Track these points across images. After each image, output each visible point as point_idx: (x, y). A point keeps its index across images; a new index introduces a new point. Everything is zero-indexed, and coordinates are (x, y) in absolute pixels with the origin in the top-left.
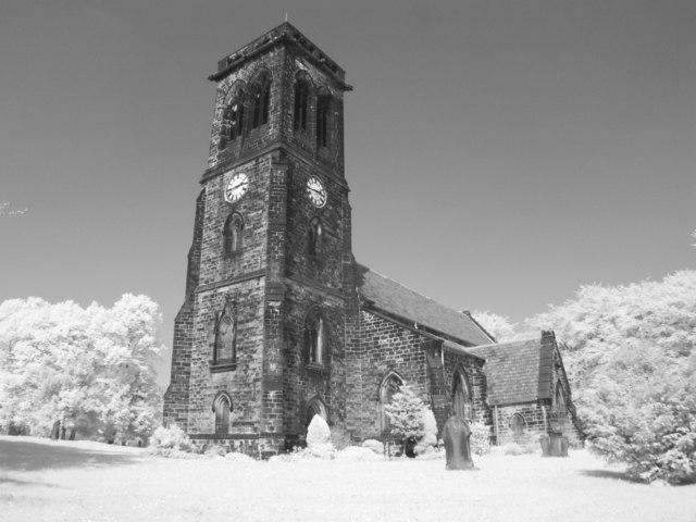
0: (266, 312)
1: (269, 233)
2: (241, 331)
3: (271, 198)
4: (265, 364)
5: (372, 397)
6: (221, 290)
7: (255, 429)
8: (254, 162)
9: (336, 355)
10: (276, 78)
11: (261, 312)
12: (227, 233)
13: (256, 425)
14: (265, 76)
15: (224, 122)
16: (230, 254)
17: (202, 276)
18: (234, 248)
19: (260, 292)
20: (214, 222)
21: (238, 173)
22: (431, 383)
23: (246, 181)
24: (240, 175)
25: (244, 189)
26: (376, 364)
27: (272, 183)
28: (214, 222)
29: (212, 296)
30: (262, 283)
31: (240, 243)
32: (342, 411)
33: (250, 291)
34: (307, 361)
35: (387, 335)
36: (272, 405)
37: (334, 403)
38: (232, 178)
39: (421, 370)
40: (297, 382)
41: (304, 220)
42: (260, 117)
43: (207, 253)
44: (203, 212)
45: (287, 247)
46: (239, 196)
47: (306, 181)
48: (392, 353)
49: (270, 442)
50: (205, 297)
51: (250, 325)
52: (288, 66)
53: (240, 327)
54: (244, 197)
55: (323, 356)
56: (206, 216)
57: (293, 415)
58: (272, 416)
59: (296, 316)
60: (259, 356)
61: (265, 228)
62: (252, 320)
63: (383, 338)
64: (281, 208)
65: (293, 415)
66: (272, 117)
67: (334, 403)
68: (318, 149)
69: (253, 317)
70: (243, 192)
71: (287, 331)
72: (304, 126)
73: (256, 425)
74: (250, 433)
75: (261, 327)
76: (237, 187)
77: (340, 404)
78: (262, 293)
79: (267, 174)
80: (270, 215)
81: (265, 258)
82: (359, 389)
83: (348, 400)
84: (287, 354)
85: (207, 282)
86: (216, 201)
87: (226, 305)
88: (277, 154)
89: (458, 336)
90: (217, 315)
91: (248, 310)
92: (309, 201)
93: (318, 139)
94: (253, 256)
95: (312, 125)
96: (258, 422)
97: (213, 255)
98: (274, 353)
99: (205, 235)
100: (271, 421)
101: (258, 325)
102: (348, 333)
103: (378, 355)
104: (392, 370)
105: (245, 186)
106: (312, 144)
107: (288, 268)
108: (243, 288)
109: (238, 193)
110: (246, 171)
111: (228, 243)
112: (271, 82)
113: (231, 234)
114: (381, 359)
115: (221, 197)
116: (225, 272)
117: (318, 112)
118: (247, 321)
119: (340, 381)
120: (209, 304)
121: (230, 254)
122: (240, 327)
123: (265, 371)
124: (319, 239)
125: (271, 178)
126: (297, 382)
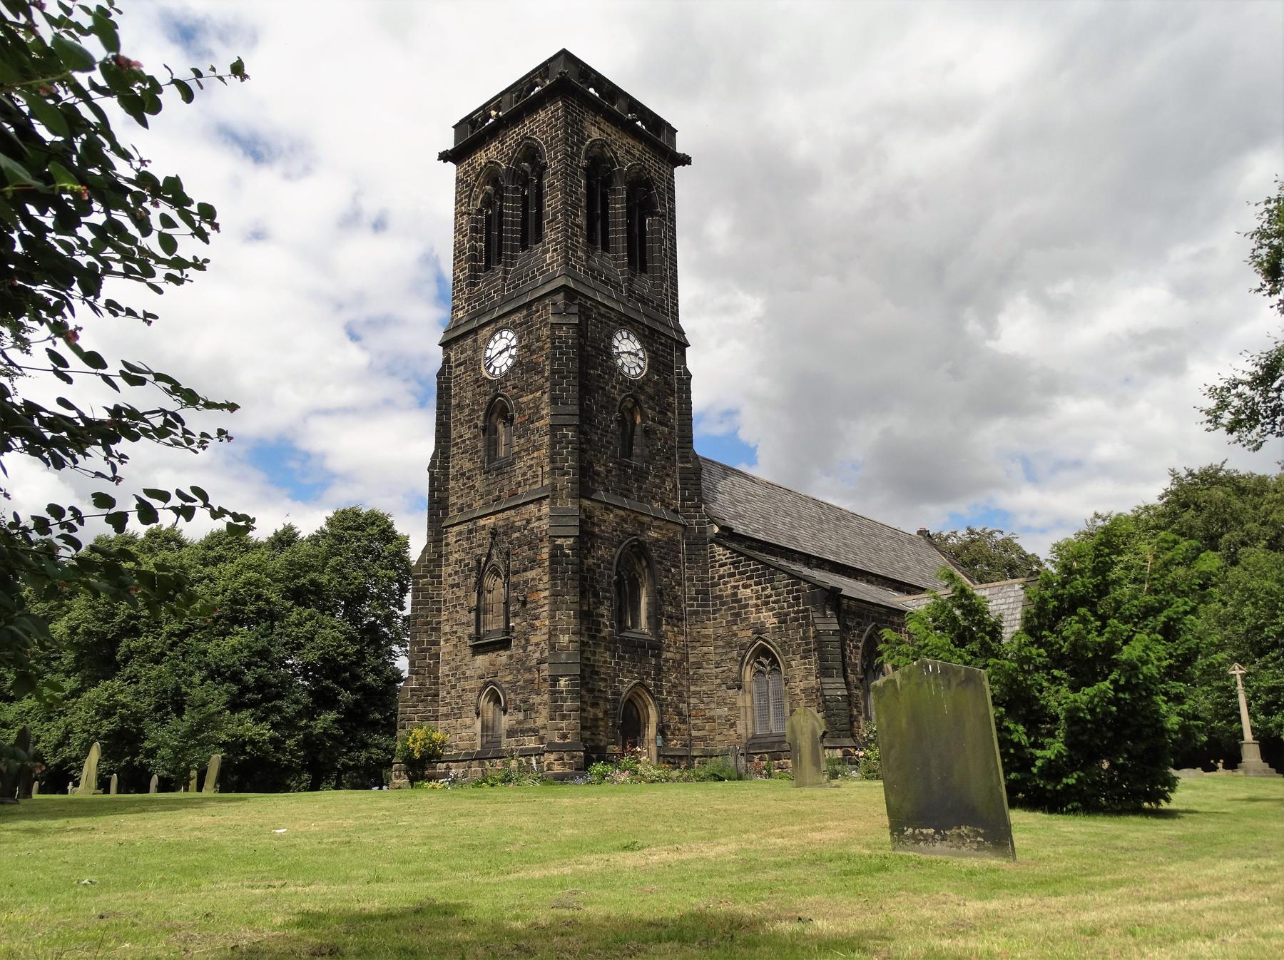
0: (553, 556)
1: (554, 428)
2: (516, 586)
3: (553, 372)
4: (552, 634)
5: (730, 683)
6: (482, 522)
7: (541, 740)
8: (525, 312)
9: (670, 617)
10: (553, 162)
11: (545, 553)
12: (489, 431)
13: (542, 732)
14: (530, 152)
15: (472, 238)
16: (495, 465)
17: (453, 499)
18: (502, 452)
19: (541, 523)
20: (467, 411)
21: (499, 330)
22: (820, 659)
23: (514, 343)
24: (505, 333)
25: (511, 356)
26: (735, 628)
27: (554, 347)
28: (467, 411)
29: (470, 531)
30: (546, 509)
31: (509, 444)
32: (683, 706)
33: (528, 522)
34: (622, 626)
35: (752, 582)
36: (565, 700)
37: (669, 693)
38: (492, 337)
39: (805, 638)
40: (604, 659)
41: (609, 404)
42: (531, 232)
43: (461, 463)
44: (450, 397)
45: (583, 449)
46: (504, 369)
47: (610, 337)
48: (758, 611)
49: (562, 759)
50: (460, 533)
51: (530, 574)
52: (573, 130)
53: (514, 579)
54: (512, 369)
55: (648, 618)
56: (453, 402)
57: (601, 715)
58: (563, 717)
59: (601, 558)
60: (544, 622)
61: (547, 420)
62: (532, 568)
63: (745, 587)
64: (571, 388)
65: (601, 715)
66: (549, 234)
67: (669, 693)
68: (630, 281)
69: (534, 562)
70: (510, 362)
71: (586, 584)
72: (606, 248)
73: (542, 732)
74: (532, 745)
75: (546, 578)
76: (501, 353)
77: (680, 694)
78: (545, 524)
79: (546, 332)
80: (554, 400)
81: (547, 469)
82: (710, 669)
83: (692, 688)
84: (587, 619)
85: (461, 510)
86: (469, 377)
87: (491, 546)
88: (560, 298)
89: (897, 577)
90: (479, 561)
91: (525, 552)
92: (614, 370)
93: (631, 262)
94: (531, 467)
95: (619, 237)
96: (544, 727)
97: (468, 465)
98: (566, 617)
99: (454, 434)
100: (563, 724)
101: (539, 576)
102: (690, 579)
103: (738, 615)
104: (760, 638)
105: (513, 352)
106: (620, 274)
107: (583, 490)
108: (517, 518)
109: (502, 363)
110: (514, 327)
111: (492, 446)
112: (544, 167)
113: (496, 431)
114: (743, 620)
115: (476, 369)
116: (489, 493)
117: (630, 214)
118: (525, 570)
119: (678, 657)
120: (465, 544)
121: (495, 465)
122: (514, 579)
123: (552, 647)
124: (638, 430)
125: (553, 338)
126: (604, 659)
